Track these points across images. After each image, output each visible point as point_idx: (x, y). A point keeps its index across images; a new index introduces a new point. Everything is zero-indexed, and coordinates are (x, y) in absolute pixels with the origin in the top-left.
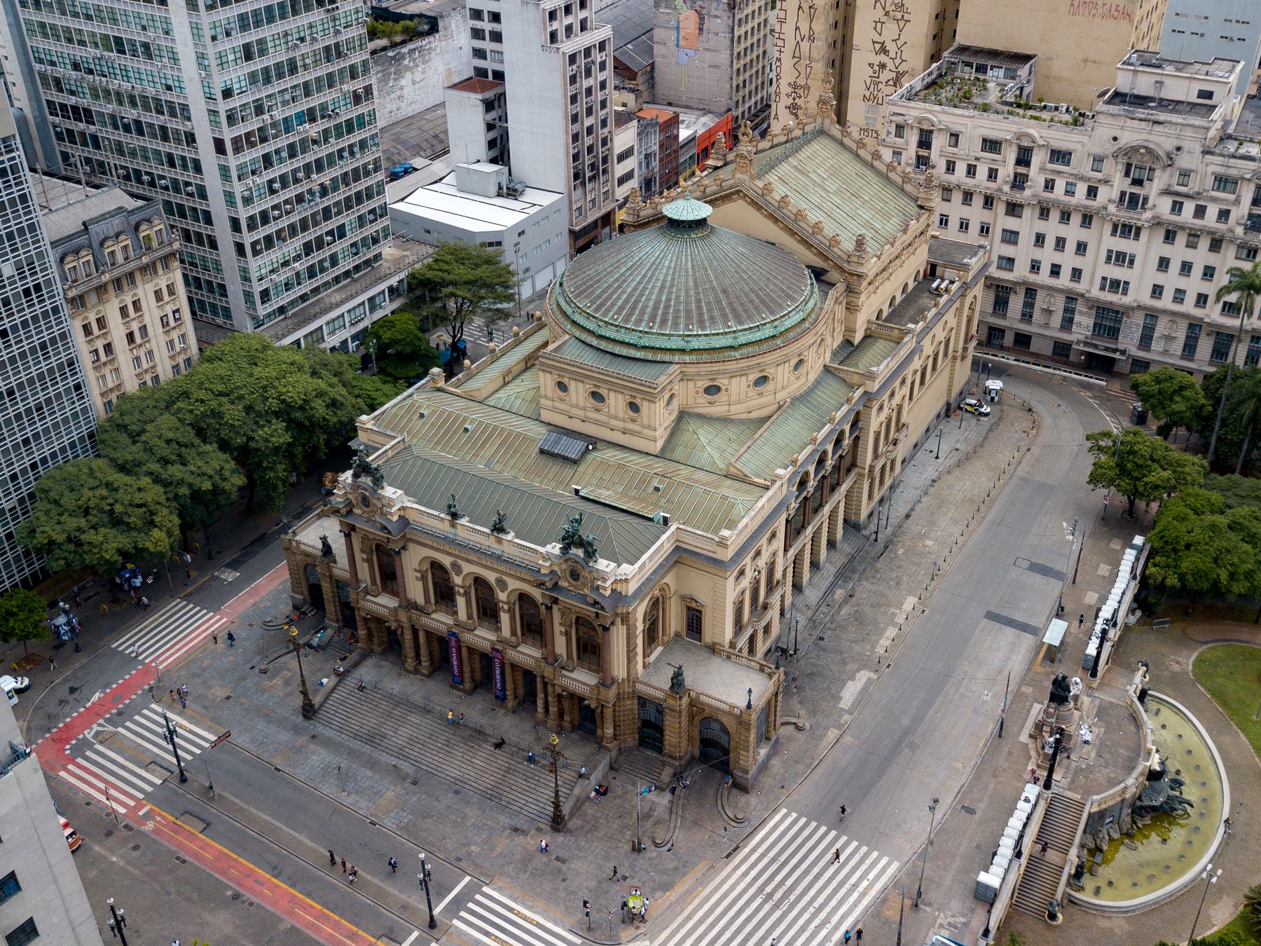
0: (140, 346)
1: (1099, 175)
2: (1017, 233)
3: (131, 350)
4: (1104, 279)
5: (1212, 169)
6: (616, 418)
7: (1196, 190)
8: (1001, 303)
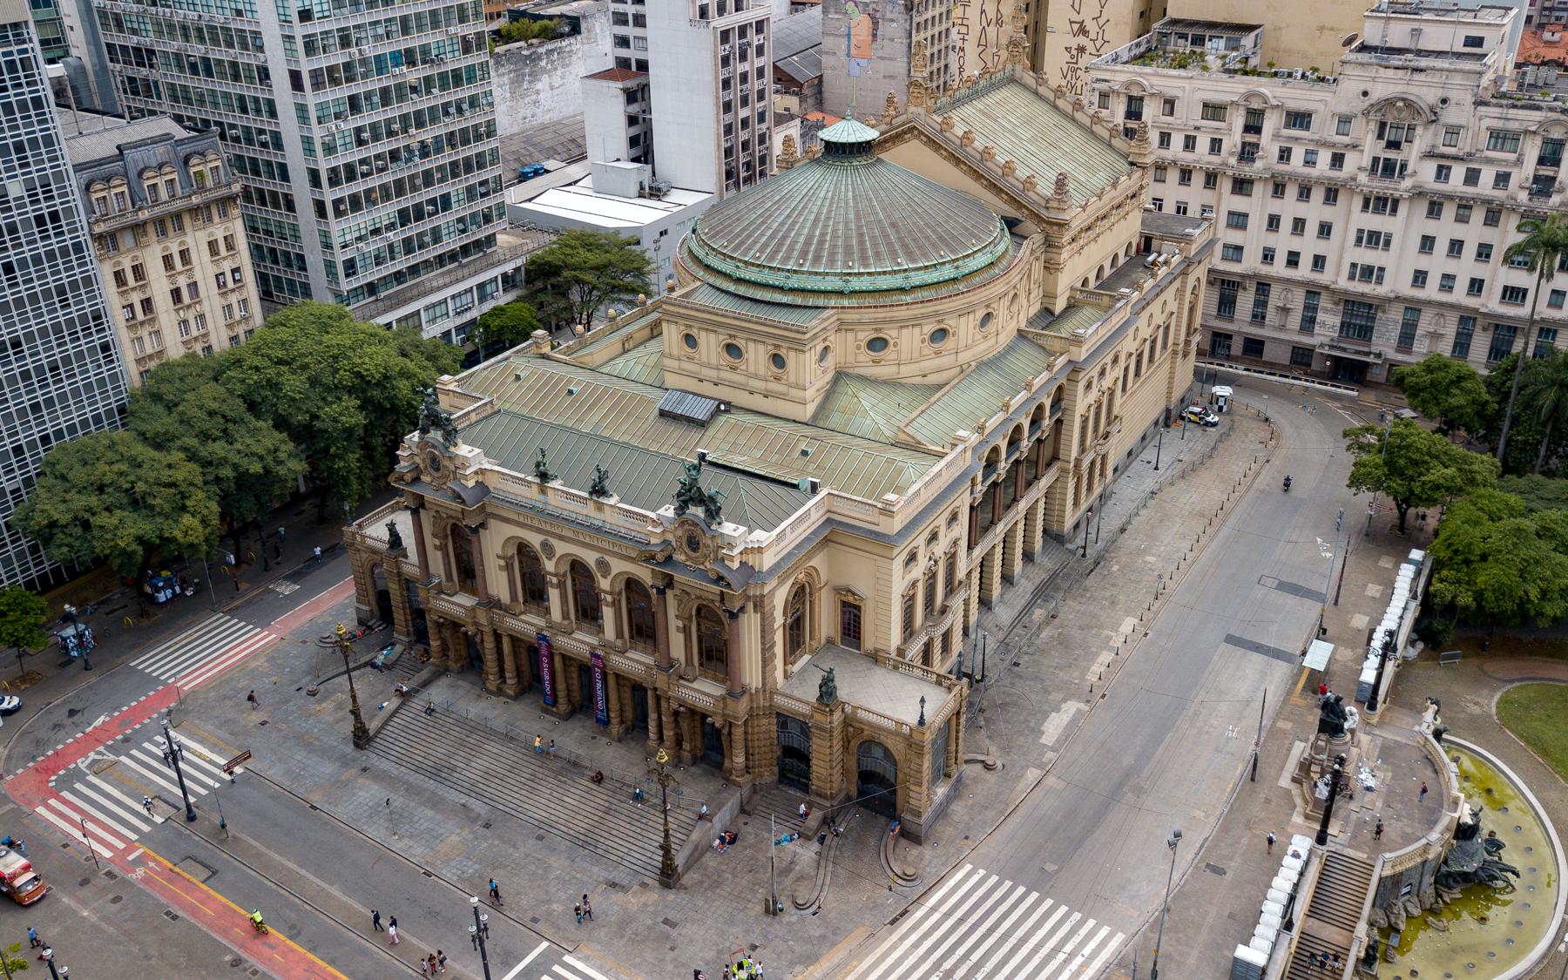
0: (189, 307)
1: (1345, 140)
2: (1246, 216)
3: (177, 311)
4: (1354, 265)
5: (1486, 123)
6: (756, 376)
7: (1467, 150)
8: (1226, 304)
